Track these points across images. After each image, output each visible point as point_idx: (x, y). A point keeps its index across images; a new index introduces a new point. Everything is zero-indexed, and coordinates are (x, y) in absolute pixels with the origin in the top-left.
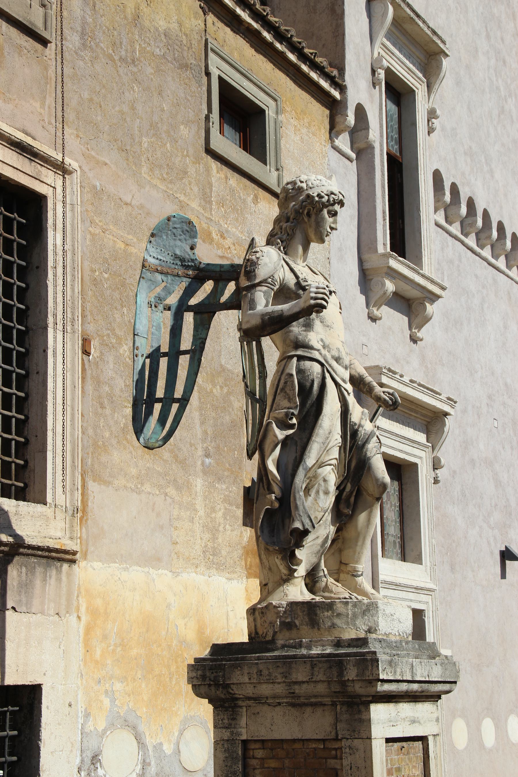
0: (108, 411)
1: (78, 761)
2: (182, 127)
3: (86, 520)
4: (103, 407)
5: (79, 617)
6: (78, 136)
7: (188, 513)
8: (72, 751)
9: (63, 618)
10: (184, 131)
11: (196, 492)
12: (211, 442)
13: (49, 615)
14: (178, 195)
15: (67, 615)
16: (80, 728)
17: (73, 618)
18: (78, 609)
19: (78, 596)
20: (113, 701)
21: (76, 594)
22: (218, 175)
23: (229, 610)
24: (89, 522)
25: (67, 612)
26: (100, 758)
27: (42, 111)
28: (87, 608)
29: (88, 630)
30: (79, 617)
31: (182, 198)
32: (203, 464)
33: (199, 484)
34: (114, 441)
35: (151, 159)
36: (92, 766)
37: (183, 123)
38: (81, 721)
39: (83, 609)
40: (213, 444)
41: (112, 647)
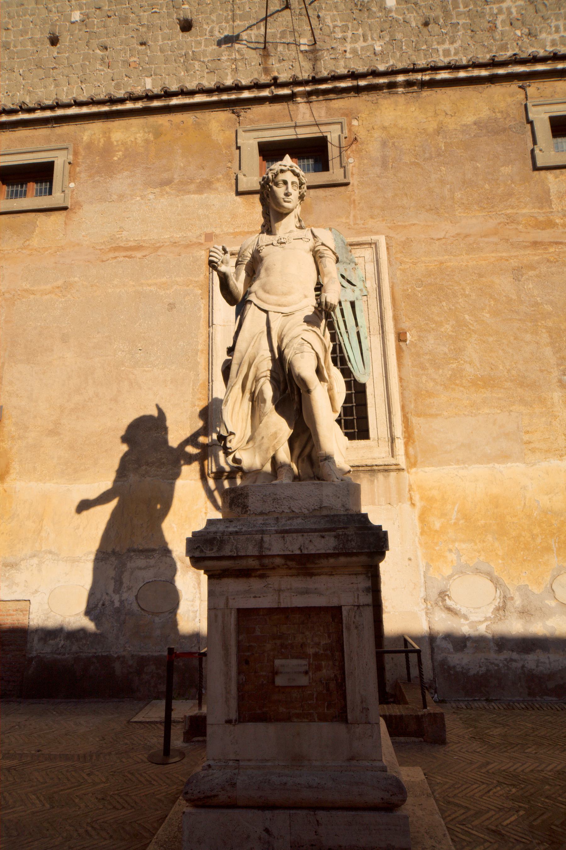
0: (431, 371)
1: (422, 594)
2: (503, 168)
4: (424, 368)
5: (413, 505)
6: (383, 220)
7: (544, 419)
8: (415, 588)
9: (395, 506)
10: (506, 170)
11: (553, 404)
13: (381, 505)
14: (503, 212)
15: (400, 504)
16: (422, 573)
17: (407, 506)
19: (409, 491)
20: (459, 557)
21: (407, 490)
22: (557, 180)
24: (416, 443)
25: (400, 502)
26: (448, 593)
27: (348, 221)
28: (422, 498)
30: (413, 505)
31: (509, 211)
35: (466, 202)
36: (440, 599)
38: (422, 569)
39: (417, 498)
41: (453, 521)
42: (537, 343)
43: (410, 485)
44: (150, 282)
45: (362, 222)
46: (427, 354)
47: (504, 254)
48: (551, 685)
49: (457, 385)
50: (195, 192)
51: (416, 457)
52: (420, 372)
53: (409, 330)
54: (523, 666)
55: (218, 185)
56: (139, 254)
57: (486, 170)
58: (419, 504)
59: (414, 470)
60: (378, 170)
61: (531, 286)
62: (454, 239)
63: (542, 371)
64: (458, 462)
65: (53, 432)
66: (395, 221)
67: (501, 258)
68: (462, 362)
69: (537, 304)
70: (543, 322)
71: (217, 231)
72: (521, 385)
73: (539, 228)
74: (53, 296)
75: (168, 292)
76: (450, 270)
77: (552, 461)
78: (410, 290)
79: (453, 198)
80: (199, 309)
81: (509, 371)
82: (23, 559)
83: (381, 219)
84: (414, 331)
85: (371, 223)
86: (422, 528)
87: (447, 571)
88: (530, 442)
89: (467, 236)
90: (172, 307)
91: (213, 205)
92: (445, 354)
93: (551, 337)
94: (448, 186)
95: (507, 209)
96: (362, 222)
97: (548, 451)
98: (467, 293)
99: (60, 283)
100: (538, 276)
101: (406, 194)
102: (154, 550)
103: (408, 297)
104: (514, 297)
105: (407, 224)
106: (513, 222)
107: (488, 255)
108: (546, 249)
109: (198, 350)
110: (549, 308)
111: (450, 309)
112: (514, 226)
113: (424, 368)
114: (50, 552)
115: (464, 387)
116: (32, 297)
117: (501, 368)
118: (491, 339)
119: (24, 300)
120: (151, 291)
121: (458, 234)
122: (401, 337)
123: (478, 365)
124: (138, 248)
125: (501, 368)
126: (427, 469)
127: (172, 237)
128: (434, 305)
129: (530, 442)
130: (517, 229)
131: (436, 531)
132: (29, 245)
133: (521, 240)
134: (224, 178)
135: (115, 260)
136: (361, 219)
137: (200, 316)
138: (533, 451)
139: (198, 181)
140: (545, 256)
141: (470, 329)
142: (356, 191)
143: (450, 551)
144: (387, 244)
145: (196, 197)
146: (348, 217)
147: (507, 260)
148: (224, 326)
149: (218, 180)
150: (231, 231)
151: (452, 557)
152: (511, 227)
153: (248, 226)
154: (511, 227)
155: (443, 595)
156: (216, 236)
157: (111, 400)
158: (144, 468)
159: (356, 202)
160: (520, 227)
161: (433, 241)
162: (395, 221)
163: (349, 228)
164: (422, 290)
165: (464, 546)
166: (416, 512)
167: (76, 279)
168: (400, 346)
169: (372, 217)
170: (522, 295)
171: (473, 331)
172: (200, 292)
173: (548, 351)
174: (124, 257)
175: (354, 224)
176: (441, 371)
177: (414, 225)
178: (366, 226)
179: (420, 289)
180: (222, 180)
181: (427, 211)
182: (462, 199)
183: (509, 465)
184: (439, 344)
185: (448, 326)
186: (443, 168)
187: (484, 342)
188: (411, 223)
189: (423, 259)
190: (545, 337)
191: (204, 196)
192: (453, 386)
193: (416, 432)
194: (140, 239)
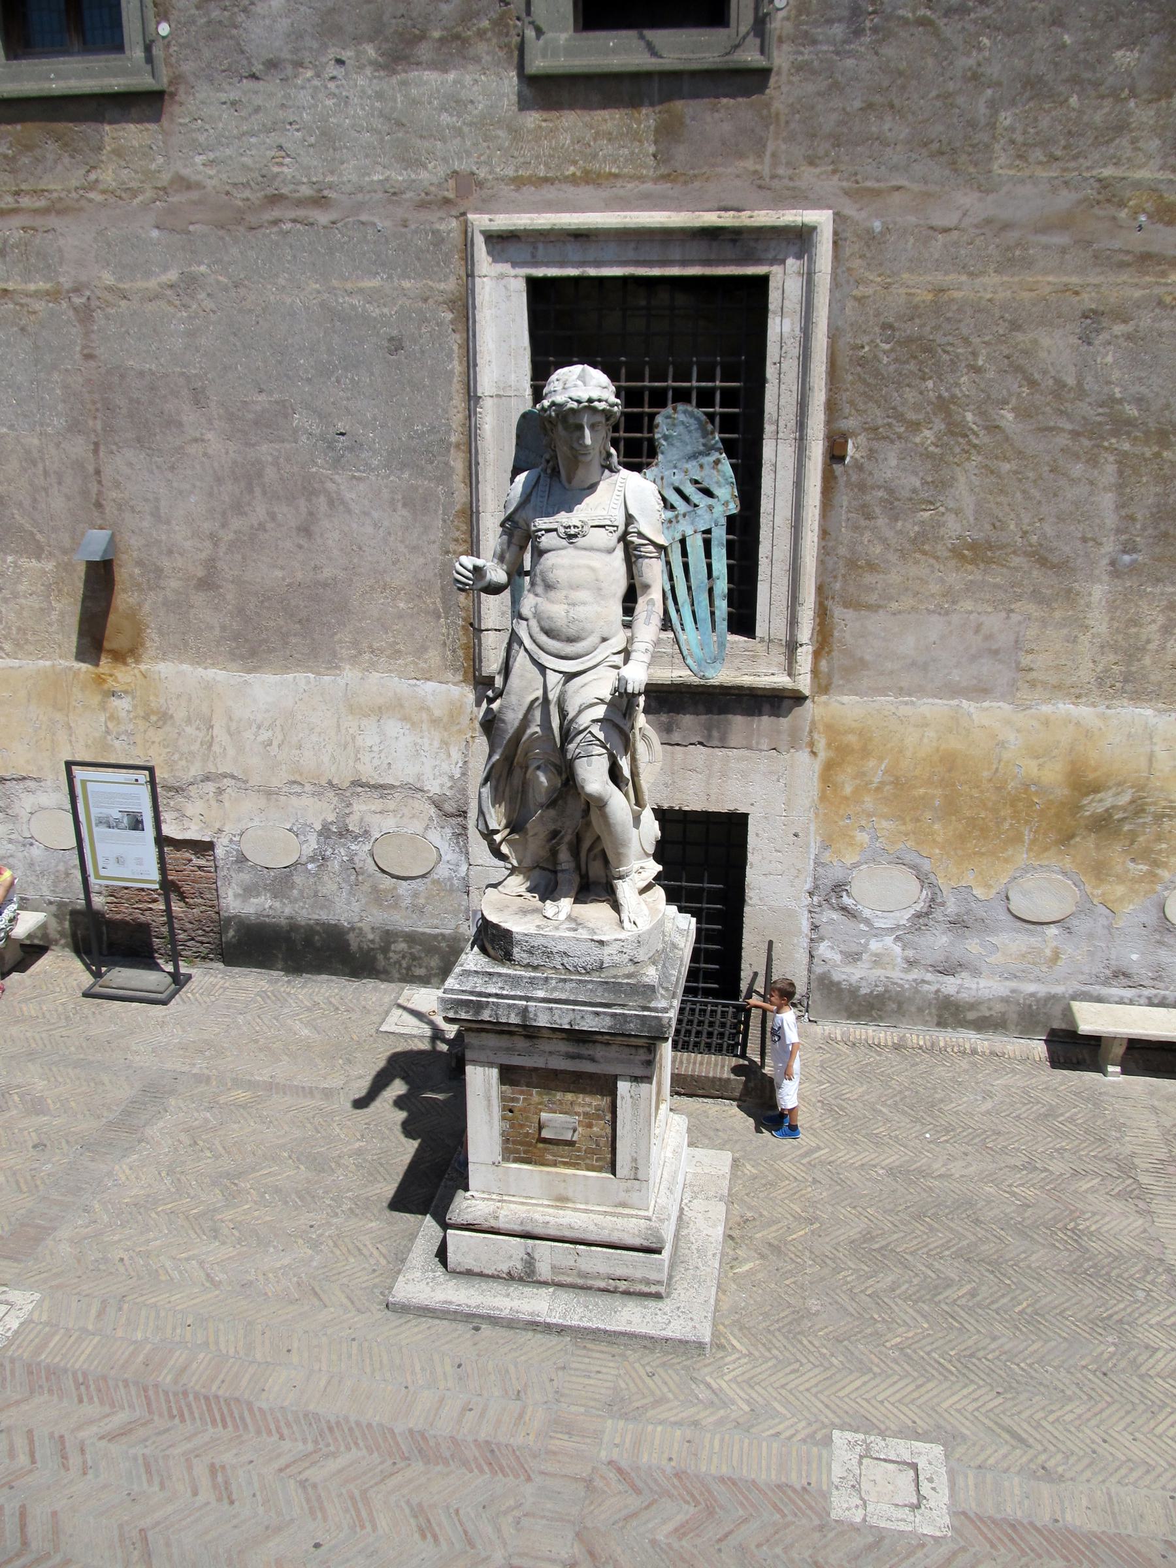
0: (882, 522)
1: (808, 886)
2: (1119, 53)
3: (829, 653)
4: (869, 517)
5: (814, 754)
6: (834, 172)
10: (1125, 58)
11: (1088, 605)
12: (1144, 529)
14: (1094, 173)
17: (803, 756)
18: (811, 744)
19: (811, 732)
23: (1156, 748)
27: (758, 167)
28: (829, 745)
29: (829, 768)
30: (814, 754)
31: (1107, 172)
32: (1113, 563)
33: (1099, 592)
34: (893, 557)
35: (1020, 139)
37: (1120, 47)
38: (813, 851)
39: (821, 744)
40: (1150, 531)
42: (1092, 483)
43: (813, 723)
44: (349, 286)
45: (790, 172)
46: (879, 487)
47: (1074, 280)
48: (971, 1016)
49: (925, 553)
50: (434, 65)
51: (830, 676)
52: (863, 523)
53: (854, 434)
54: (938, 991)
55: (481, 48)
56: (322, 217)
57: (1082, 55)
58: (823, 755)
59: (824, 698)
60: (838, 30)
61: (1109, 359)
62: (978, 231)
63: (1084, 540)
64: (901, 691)
65: (207, 583)
66: (859, 177)
67: (1066, 288)
68: (942, 509)
69: (1112, 401)
70: (1114, 441)
71: (482, 173)
72: (1043, 562)
73: (1161, 220)
74: (162, 304)
75: (386, 310)
76: (955, 308)
77: (1061, 705)
78: (867, 349)
79: (992, 126)
80: (450, 357)
81: (1025, 534)
82: (192, 784)
83: (831, 168)
84: (862, 439)
85: (808, 176)
86: (823, 792)
87: (850, 859)
88: (1031, 669)
89: (1006, 226)
90: (396, 345)
91: (472, 102)
92: (914, 491)
93: (1120, 473)
94: (989, 92)
95: (1105, 166)
96: (790, 172)
97: (1058, 687)
98: (980, 363)
99: (172, 276)
100: (1129, 337)
101: (892, 106)
102: (393, 787)
103: (862, 362)
104: (1071, 381)
105: (882, 185)
106: (1108, 201)
107: (1040, 278)
108: (1163, 274)
109: (450, 444)
110: (1131, 411)
111: (940, 397)
112: (1112, 210)
113: (869, 517)
114: (233, 777)
115: (937, 558)
116: (123, 303)
117: (1012, 527)
118: (1006, 467)
119: (109, 310)
120: (353, 307)
121: (988, 222)
122: (835, 455)
123: (971, 519)
124: (320, 201)
125: (1012, 527)
126: (845, 699)
127: (387, 179)
128: (909, 385)
129: (1031, 669)
130: (1114, 218)
131: (846, 798)
132: (97, 181)
133: (1117, 247)
134: (493, 30)
135: (275, 229)
136: (788, 164)
137: (452, 371)
138: (1033, 684)
139: (437, 34)
140: (1157, 291)
141: (969, 443)
142: (784, 89)
143: (862, 828)
144: (835, 233)
145: (431, 77)
146: (760, 155)
147: (1077, 293)
148: (498, 396)
149: (481, 34)
150: (510, 172)
151: (863, 837)
152: (1101, 213)
153: (546, 164)
154: (1101, 213)
155: (839, 888)
156: (480, 184)
157: (299, 529)
158: (367, 656)
159: (783, 118)
160: (1123, 214)
161: (931, 232)
162: (859, 177)
163: (760, 187)
164: (892, 350)
165: (885, 824)
166: (817, 765)
167: (203, 268)
168: (832, 471)
169: (812, 162)
170: (1089, 378)
171: (975, 446)
172: (449, 316)
173: (1107, 500)
174: (294, 221)
175: (773, 177)
176: (900, 524)
177: (898, 188)
178: (797, 183)
179: (887, 347)
180: (489, 34)
181: (932, 156)
182: (1012, 129)
183: (986, 704)
184: (904, 470)
185: (927, 433)
186: (985, 41)
187: (992, 472)
188: (894, 183)
189: (905, 276)
190: (1109, 471)
191: (451, 76)
192: (918, 555)
193: (836, 634)
194: (321, 178)
